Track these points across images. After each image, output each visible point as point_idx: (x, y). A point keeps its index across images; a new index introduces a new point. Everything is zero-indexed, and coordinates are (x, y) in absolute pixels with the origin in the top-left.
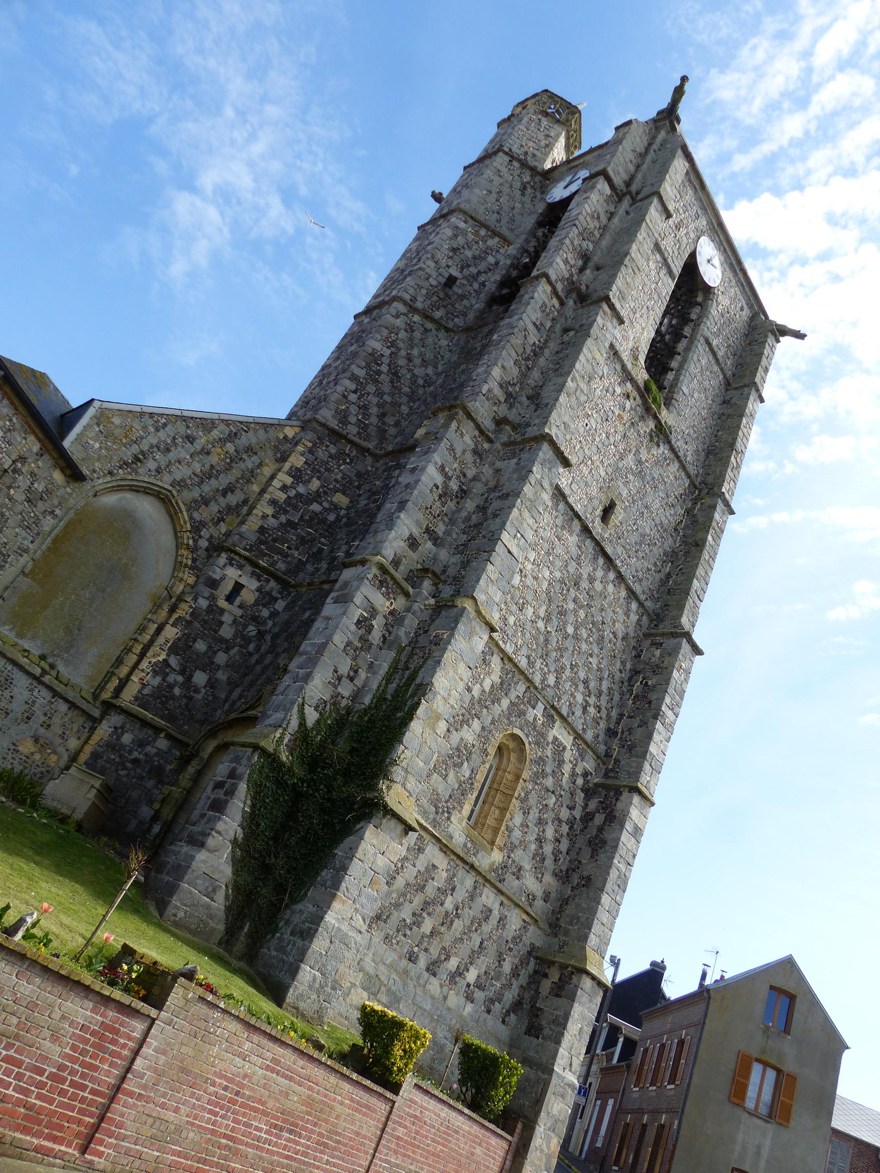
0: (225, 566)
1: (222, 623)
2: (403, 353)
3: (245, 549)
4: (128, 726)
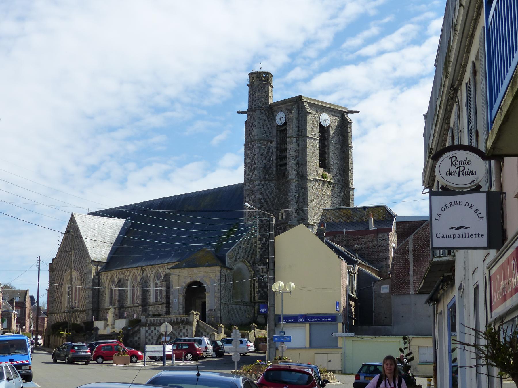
2: (265, 195)
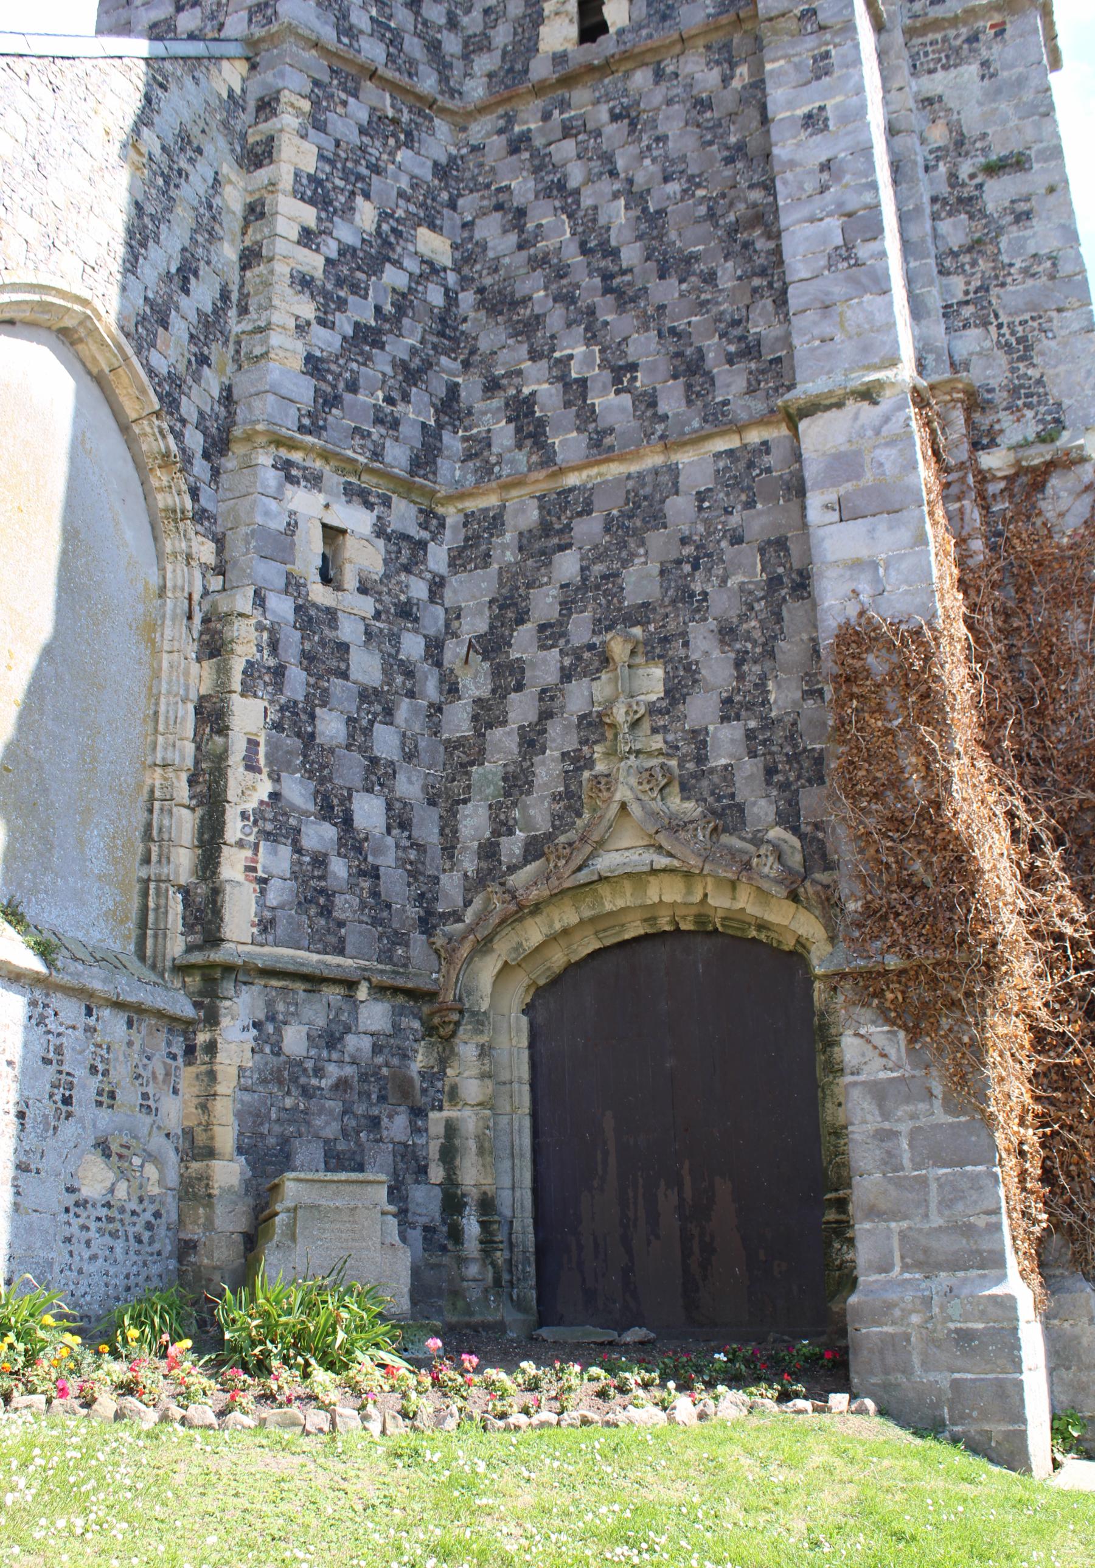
0: (280, 488)
1: (343, 648)
3: (301, 429)
4: (281, 1007)
